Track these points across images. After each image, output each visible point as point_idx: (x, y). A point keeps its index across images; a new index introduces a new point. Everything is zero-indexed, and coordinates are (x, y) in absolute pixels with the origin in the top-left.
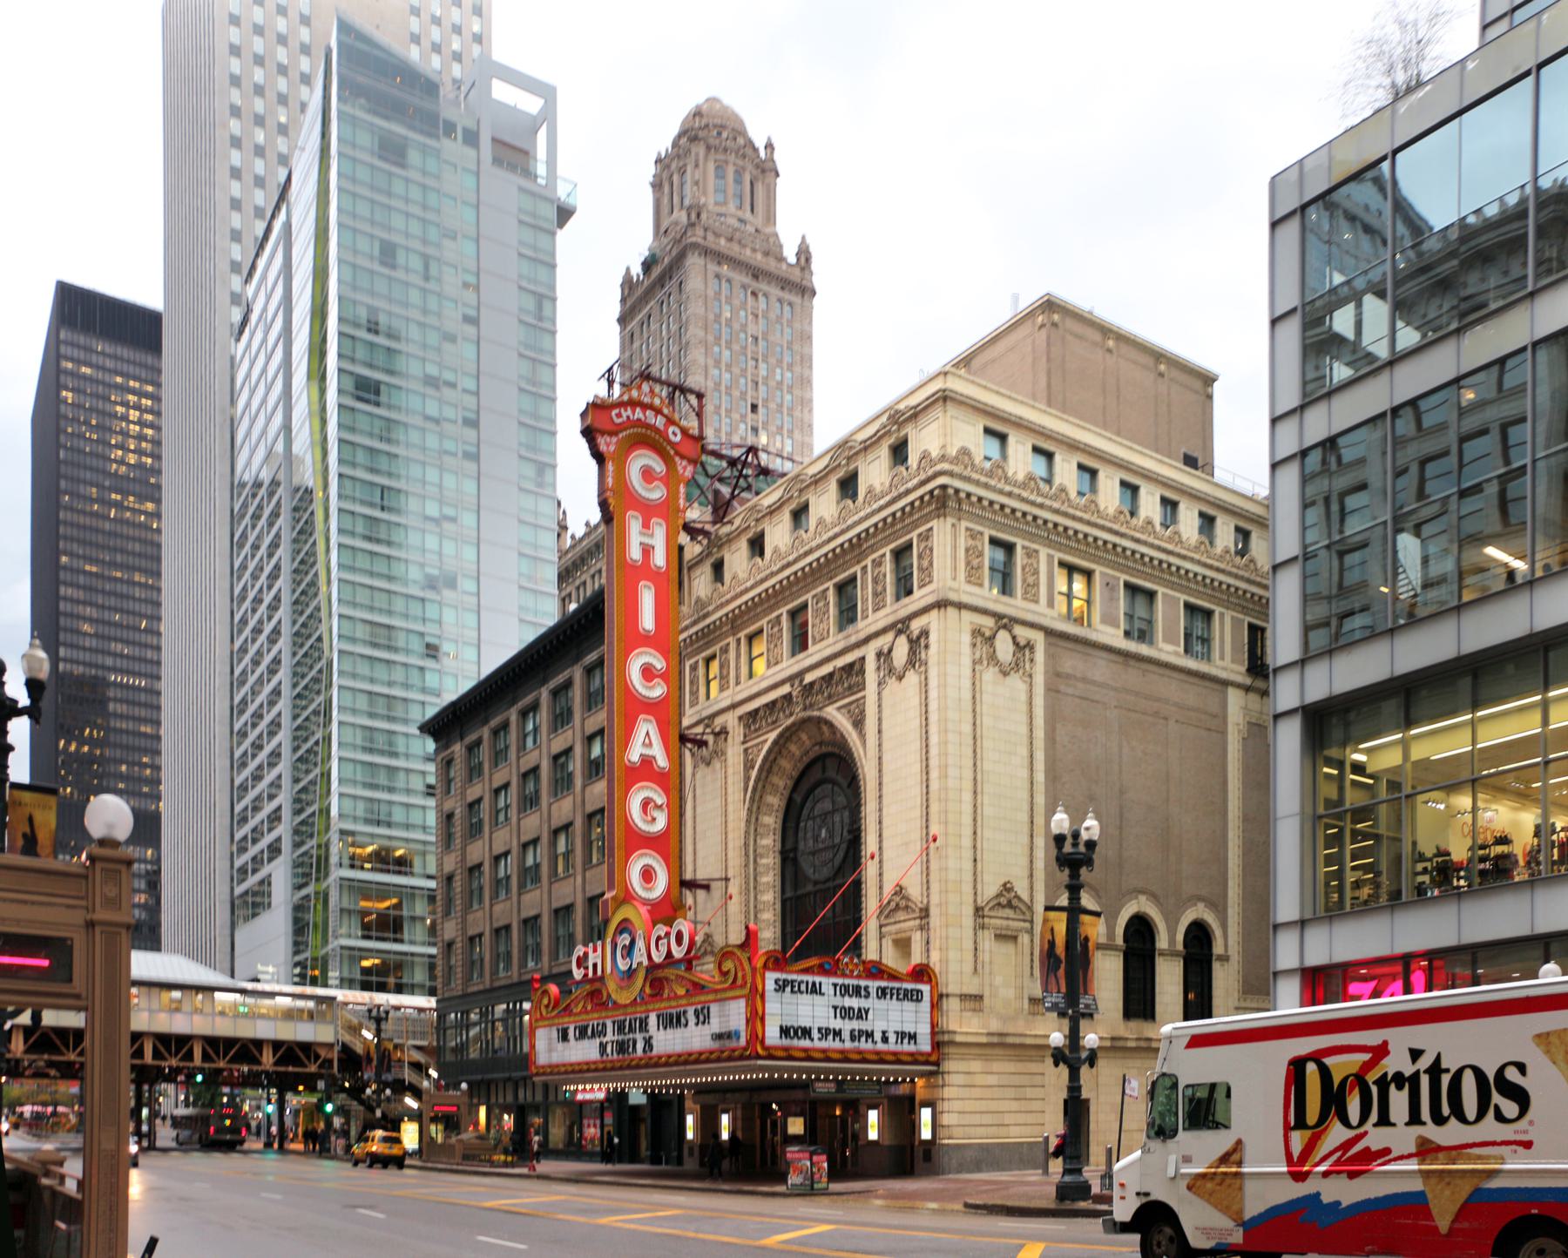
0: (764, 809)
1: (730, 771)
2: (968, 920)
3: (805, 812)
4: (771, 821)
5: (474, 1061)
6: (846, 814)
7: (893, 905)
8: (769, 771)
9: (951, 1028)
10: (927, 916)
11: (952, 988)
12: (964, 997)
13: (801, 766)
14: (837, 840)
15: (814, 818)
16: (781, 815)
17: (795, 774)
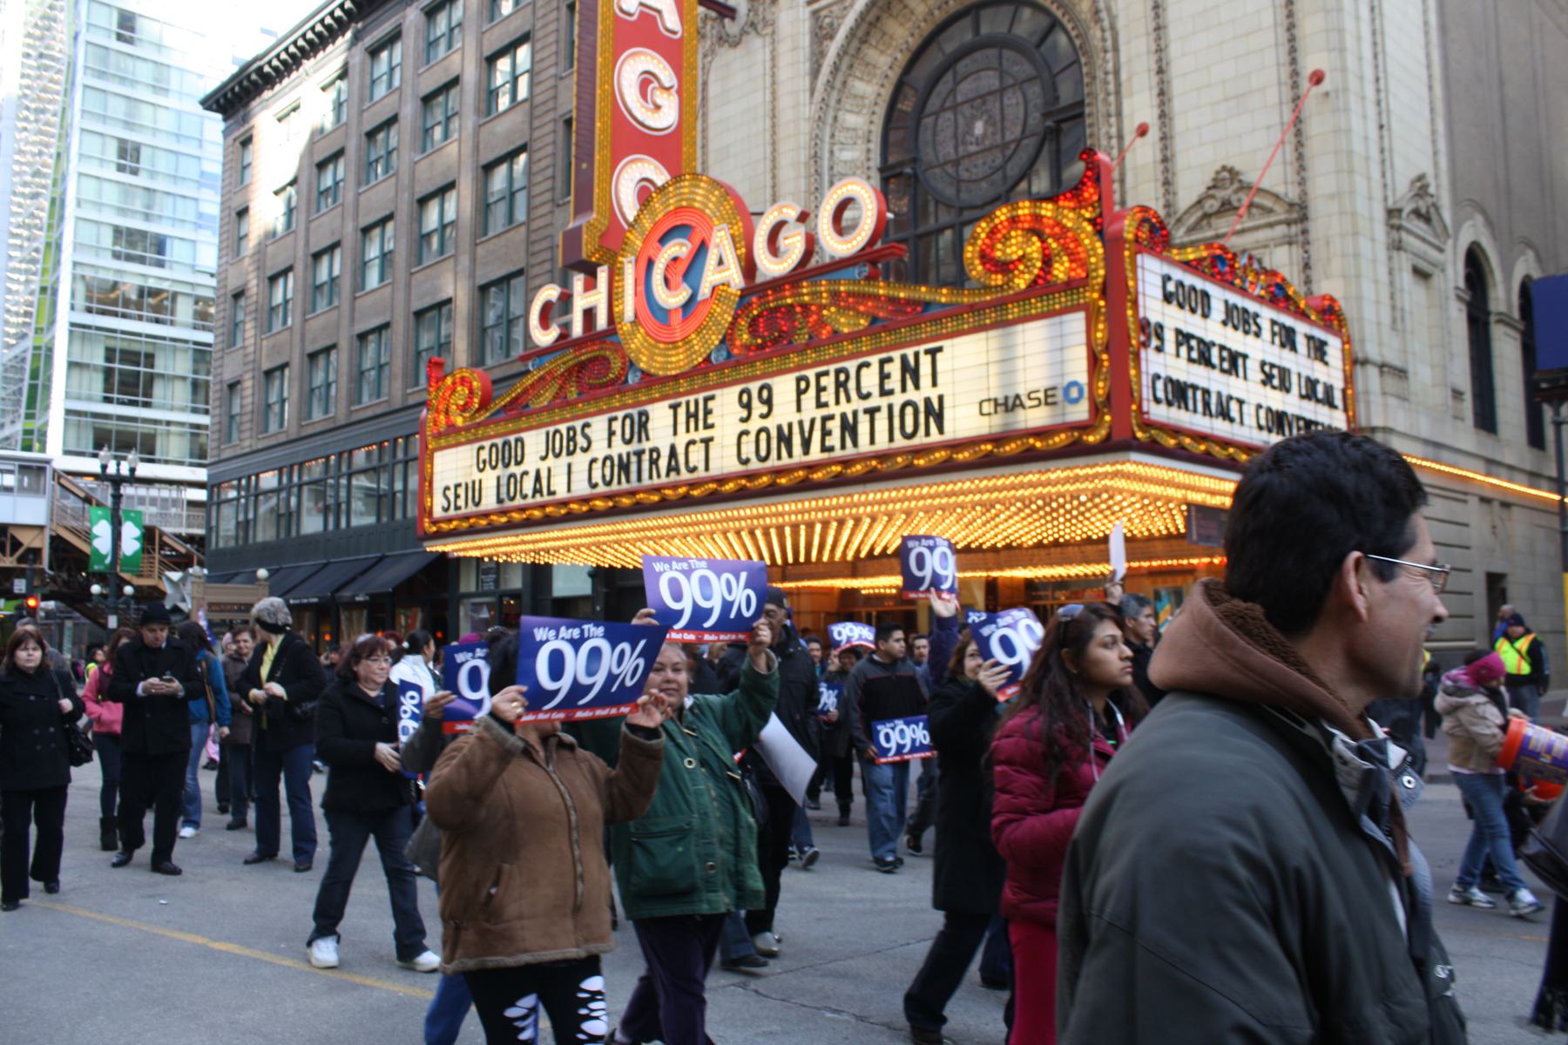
0: (847, 103)
1: (783, 47)
2: (1380, 231)
3: (934, 102)
4: (862, 119)
5: (265, 546)
6: (1034, 90)
7: (1212, 205)
8: (864, 41)
9: (1377, 421)
10: (1304, 218)
11: (1372, 351)
12: (1382, 366)
13: (927, 28)
14: (1014, 132)
15: (955, 107)
16: (881, 110)
17: (914, 43)
